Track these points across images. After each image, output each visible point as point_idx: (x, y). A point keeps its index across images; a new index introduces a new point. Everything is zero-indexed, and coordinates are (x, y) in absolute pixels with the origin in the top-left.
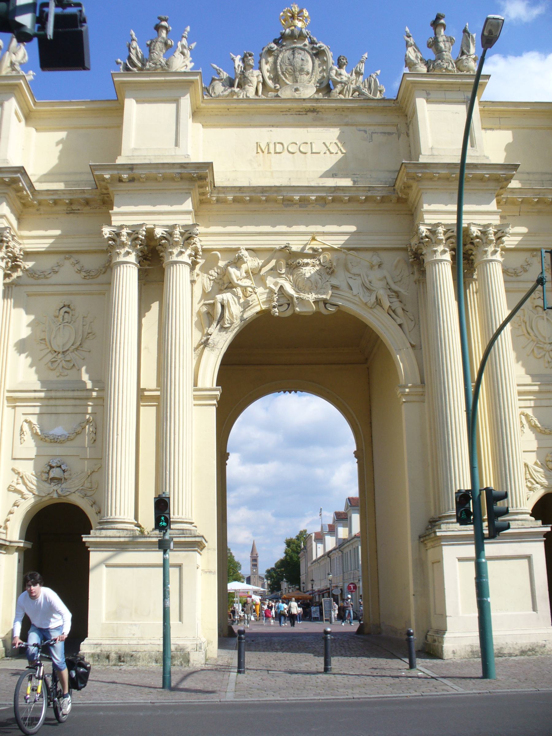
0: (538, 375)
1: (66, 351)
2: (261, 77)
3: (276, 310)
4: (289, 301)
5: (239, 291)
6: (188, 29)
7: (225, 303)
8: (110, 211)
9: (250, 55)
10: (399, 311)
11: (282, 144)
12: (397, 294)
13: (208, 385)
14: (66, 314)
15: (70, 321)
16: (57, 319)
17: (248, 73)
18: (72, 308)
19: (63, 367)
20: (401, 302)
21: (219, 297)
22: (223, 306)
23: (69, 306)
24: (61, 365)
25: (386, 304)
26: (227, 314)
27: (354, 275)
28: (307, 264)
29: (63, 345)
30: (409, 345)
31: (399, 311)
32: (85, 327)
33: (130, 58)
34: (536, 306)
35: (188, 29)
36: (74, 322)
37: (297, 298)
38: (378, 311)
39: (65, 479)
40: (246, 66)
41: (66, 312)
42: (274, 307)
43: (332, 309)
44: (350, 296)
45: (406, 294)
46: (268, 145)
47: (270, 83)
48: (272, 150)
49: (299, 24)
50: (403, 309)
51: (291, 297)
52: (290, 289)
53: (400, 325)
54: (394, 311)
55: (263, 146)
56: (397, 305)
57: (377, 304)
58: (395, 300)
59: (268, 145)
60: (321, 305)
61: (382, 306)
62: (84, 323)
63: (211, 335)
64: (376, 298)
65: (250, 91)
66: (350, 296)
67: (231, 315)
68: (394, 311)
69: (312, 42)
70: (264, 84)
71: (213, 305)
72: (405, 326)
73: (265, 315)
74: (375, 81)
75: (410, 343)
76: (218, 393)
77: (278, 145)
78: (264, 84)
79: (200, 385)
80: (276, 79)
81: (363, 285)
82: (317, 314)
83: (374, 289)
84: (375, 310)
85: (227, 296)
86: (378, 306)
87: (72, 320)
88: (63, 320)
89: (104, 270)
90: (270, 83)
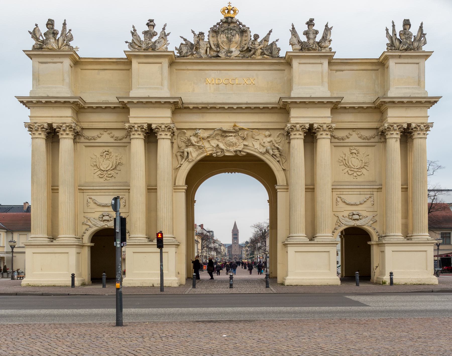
1: (108, 170)
3: (215, 154)
4: (222, 150)
7: (189, 152)
8: (128, 116)
12: (278, 149)
14: (107, 155)
15: (109, 158)
16: (102, 157)
18: (110, 152)
19: (107, 176)
20: (279, 151)
23: (108, 152)
24: (106, 176)
25: (271, 152)
29: (106, 168)
32: (117, 160)
34: (352, 153)
36: (111, 158)
37: (225, 150)
38: (267, 156)
41: (106, 154)
42: (214, 153)
43: (244, 154)
44: (253, 149)
45: (281, 149)
50: (280, 155)
52: (222, 146)
56: (277, 152)
57: (267, 152)
58: (276, 151)
61: (269, 153)
62: (117, 159)
63: (182, 164)
64: (266, 150)
66: (253, 149)
82: (236, 156)
83: (265, 146)
84: (266, 155)
85: (190, 149)
86: (267, 153)
87: (110, 157)
88: (105, 157)
89: (125, 137)
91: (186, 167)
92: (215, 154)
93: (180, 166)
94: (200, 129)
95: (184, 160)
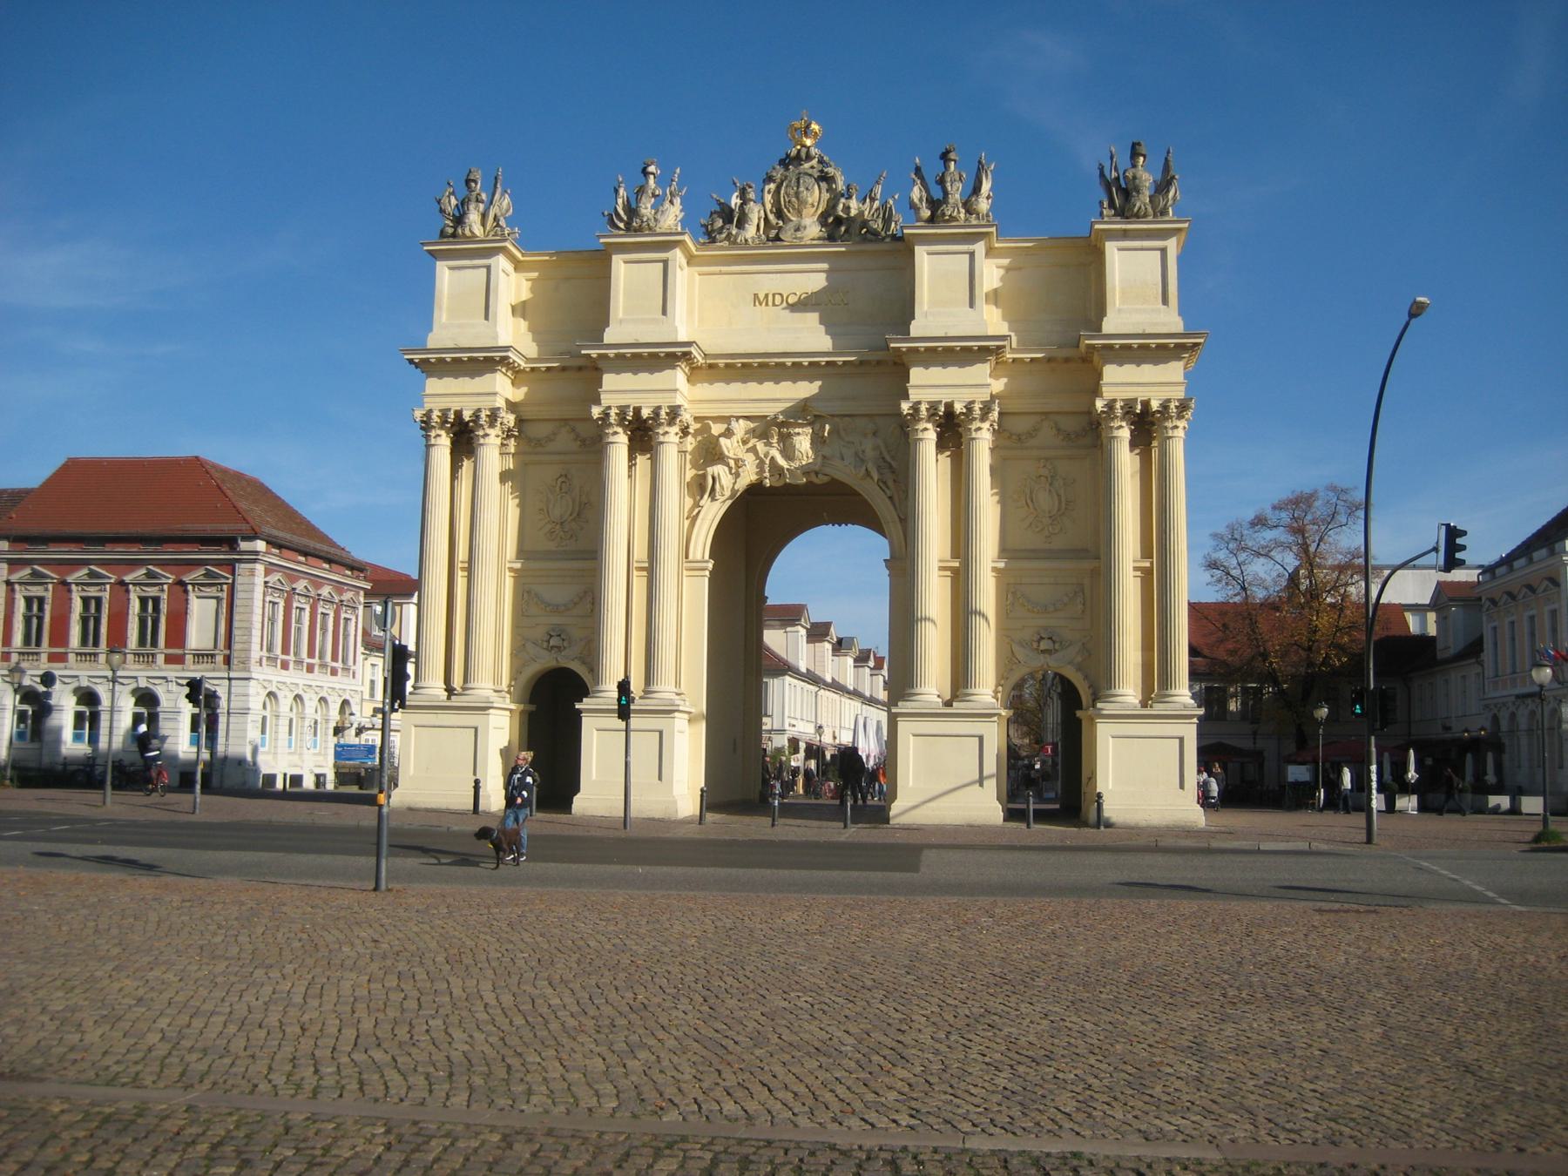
0: (1033, 551)
2: (762, 212)
5: (732, 463)
6: (678, 171)
7: (716, 475)
9: (750, 187)
10: (890, 483)
11: (780, 294)
12: (891, 466)
13: (699, 557)
17: (747, 208)
20: (893, 472)
21: (710, 470)
22: (714, 478)
26: (717, 486)
27: (848, 442)
28: (799, 434)
30: (897, 519)
31: (890, 483)
33: (616, 209)
35: (678, 171)
39: (565, 648)
40: (745, 200)
43: (826, 479)
46: (767, 296)
47: (771, 217)
48: (770, 303)
49: (808, 142)
50: (894, 481)
51: (782, 468)
53: (890, 498)
54: (885, 483)
55: (761, 297)
59: (767, 296)
60: (813, 475)
65: (750, 231)
67: (722, 487)
68: (885, 483)
69: (821, 161)
70: (766, 219)
71: (704, 476)
72: (896, 498)
73: (754, 490)
74: (890, 208)
75: (899, 517)
76: (710, 565)
77: (777, 297)
78: (766, 219)
79: (691, 557)
80: (779, 214)
81: (856, 454)
85: (719, 469)
90: (771, 217)
91: (713, 512)
92: (767, 481)
93: (699, 512)
94: (738, 418)
95: (706, 496)
